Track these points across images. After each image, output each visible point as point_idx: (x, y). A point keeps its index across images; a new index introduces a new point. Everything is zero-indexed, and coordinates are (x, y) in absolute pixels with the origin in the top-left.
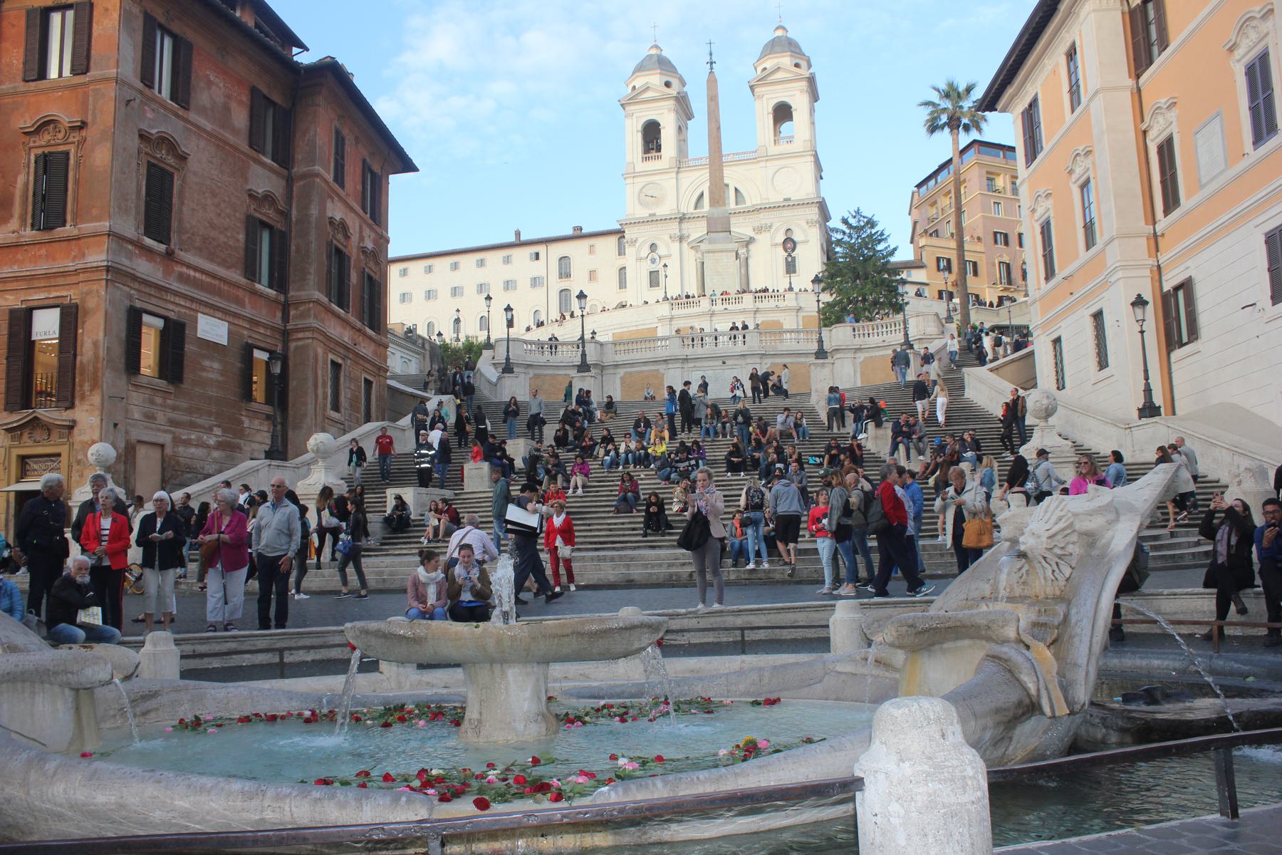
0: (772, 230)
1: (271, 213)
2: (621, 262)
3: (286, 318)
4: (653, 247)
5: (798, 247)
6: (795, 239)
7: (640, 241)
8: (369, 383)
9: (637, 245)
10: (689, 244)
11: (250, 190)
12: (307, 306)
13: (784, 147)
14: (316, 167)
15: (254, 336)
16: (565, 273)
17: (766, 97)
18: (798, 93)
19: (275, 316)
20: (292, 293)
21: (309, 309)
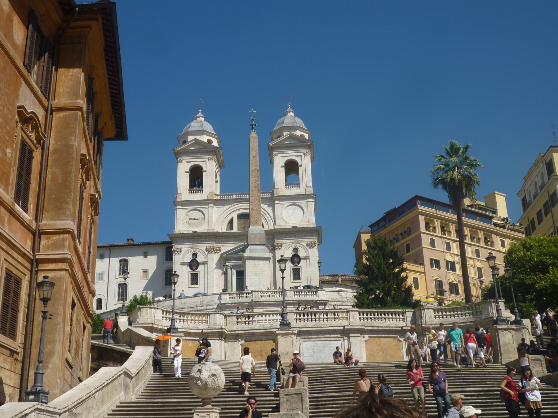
0: (282, 249)
1: (33, 136)
2: (167, 265)
3: (35, 247)
4: (195, 255)
5: (302, 261)
6: (300, 256)
7: (183, 251)
8: (84, 328)
9: (182, 254)
10: (221, 256)
11: (20, 107)
12: (61, 236)
13: (293, 191)
14: (79, 101)
15: (11, 260)
16: (124, 270)
17: (279, 155)
18: (302, 154)
19: (26, 244)
20: (44, 222)
21: (64, 240)
